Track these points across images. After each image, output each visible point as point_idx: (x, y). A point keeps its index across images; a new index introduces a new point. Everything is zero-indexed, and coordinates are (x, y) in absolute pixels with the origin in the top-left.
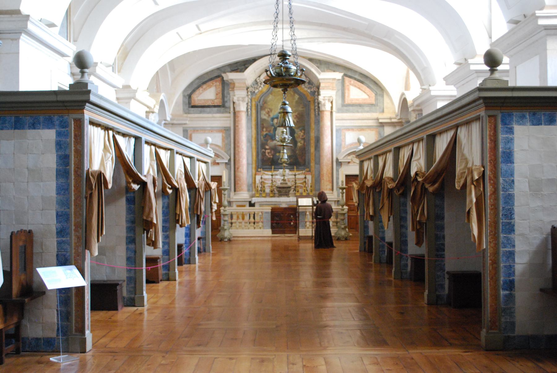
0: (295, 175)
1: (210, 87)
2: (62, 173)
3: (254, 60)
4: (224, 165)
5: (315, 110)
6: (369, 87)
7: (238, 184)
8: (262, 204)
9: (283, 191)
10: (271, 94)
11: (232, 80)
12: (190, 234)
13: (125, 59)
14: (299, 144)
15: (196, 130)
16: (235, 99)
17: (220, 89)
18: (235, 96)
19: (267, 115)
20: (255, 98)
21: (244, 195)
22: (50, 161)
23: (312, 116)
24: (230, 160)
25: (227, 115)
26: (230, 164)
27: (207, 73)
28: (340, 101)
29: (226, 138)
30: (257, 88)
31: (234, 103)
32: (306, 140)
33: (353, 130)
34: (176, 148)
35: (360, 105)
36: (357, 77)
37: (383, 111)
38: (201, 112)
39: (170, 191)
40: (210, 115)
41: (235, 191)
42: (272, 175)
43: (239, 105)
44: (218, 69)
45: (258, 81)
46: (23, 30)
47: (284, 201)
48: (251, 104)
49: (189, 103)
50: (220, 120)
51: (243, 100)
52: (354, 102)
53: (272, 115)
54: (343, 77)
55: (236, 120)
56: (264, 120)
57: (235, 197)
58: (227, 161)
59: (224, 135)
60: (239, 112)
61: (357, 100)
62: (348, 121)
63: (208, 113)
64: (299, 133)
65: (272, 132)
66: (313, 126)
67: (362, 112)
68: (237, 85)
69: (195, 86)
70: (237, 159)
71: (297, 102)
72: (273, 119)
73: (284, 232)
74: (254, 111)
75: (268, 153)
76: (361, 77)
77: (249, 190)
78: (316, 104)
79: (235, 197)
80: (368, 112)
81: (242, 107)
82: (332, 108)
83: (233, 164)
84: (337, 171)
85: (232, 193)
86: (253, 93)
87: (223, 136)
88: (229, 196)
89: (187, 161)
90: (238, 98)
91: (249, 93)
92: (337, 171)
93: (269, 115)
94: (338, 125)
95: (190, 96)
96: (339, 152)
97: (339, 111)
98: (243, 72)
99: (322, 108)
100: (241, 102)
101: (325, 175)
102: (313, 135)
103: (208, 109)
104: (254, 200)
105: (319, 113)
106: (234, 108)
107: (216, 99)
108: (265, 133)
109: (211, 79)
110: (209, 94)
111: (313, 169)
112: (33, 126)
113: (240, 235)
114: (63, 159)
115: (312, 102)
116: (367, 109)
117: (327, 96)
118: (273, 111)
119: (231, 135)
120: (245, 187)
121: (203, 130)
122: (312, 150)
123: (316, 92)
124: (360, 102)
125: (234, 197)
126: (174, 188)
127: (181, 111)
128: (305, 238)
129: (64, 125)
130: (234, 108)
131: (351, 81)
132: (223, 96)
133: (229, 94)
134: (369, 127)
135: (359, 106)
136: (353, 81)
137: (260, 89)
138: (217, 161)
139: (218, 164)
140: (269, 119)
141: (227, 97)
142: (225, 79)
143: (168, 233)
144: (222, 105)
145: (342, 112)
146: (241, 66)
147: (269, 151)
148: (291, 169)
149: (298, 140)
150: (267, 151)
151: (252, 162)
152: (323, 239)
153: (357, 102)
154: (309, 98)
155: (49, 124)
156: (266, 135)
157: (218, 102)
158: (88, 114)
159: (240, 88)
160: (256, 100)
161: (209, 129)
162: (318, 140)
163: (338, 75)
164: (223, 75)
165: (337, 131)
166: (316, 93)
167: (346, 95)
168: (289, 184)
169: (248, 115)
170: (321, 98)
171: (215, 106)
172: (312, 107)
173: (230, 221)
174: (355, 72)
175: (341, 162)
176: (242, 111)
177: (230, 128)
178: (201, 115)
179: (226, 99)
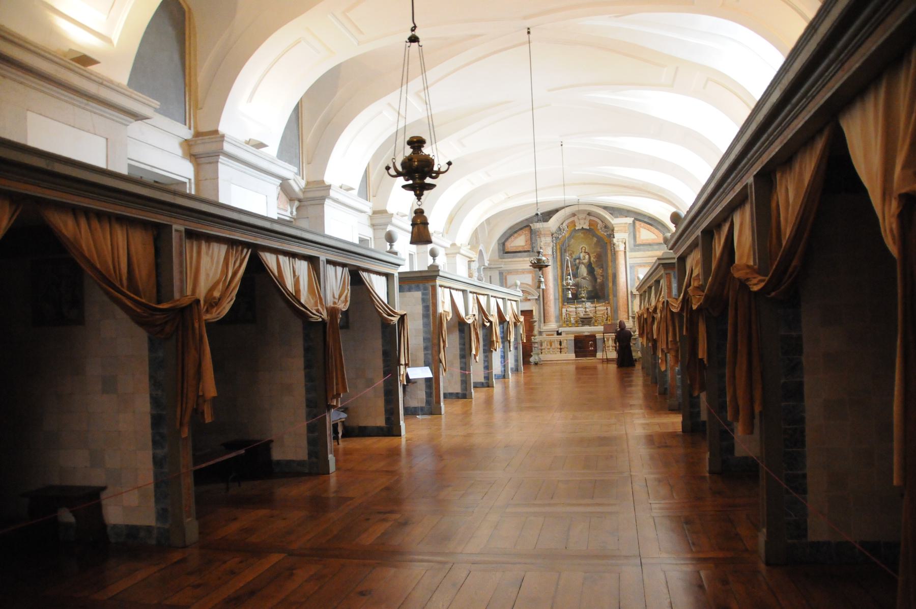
1: (520, 235)
2: (426, 316)
3: (557, 211)
6: (657, 228)
8: (567, 333)
9: (586, 321)
14: (599, 280)
15: (510, 272)
17: (529, 237)
21: (553, 325)
22: (419, 309)
23: (609, 255)
27: (517, 224)
28: (632, 242)
32: (605, 276)
34: (491, 293)
35: (650, 245)
38: (513, 257)
39: (488, 324)
44: (527, 220)
46: (390, 223)
47: (586, 330)
49: (504, 250)
51: (547, 244)
53: (574, 257)
54: (634, 222)
64: (598, 271)
66: (610, 264)
69: (508, 235)
72: (575, 260)
73: (585, 356)
77: (557, 322)
83: (542, 299)
84: (632, 302)
85: (542, 324)
86: (557, 238)
88: (540, 327)
89: (500, 302)
92: (632, 302)
95: (504, 244)
96: (632, 287)
97: (632, 250)
98: (546, 221)
99: (617, 249)
102: (610, 271)
103: (519, 254)
104: (561, 330)
105: (615, 254)
109: (521, 229)
110: (520, 242)
111: (611, 302)
112: (409, 290)
114: (426, 308)
116: (656, 247)
117: (620, 238)
121: (516, 272)
122: (610, 285)
123: (611, 236)
124: (651, 242)
126: (491, 322)
127: (497, 258)
128: (608, 361)
129: (425, 289)
132: (532, 244)
135: (649, 245)
136: (643, 224)
146: (547, 216)
148: (592, 303)
149: (598, 277)
152: (625, 360)
154: (606, 240)
155: (418, 289)
157: (527, 248)
158: (439, 282)
159: (545, 235)
162: (615, 276)
163: (630, 220)
165: (631, 267)
168: (591, 315)
170: (615, 240)
172: (609, 247)
174: (644, 216)
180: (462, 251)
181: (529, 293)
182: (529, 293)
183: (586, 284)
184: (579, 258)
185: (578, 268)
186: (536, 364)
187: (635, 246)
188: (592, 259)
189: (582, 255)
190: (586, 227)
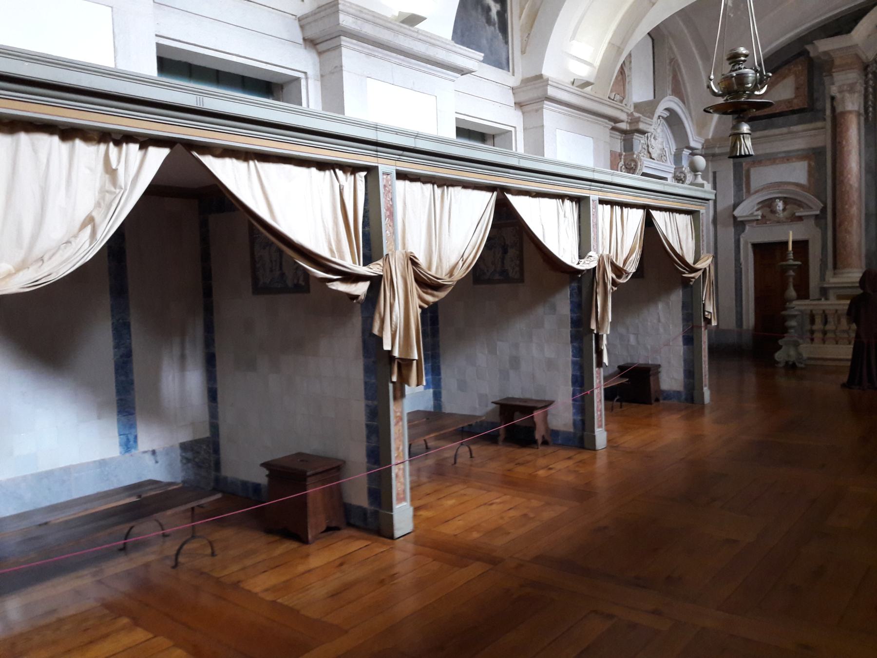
4: (812, 222)
11: (826, 53)
12: (582, 377)
13: (532, 27)
16: (834, 90)
18: (833, 84)
24: (824, 210)
25: (819, 124)
26: (826, 218)
29: (816, 172)
31: (833, 98)
40: (785, 130)
41: (835, 267)
43: (843, 100)
50: (800, 137)
51: (851, 89)
55: (838, 130)
57: (832, 280)
58: (818, 212)
59: (813, 164)
60: (844, 113)
63: (781, 127)
68: (837, 62)
70: (839, 206)
79: (832, 280)
81: (852, 104)
83: (832, 217)
87: (809, 165)
88: (823, 277)
90: (840, 87)
91: (870, 76)
98: (849, 31)
100: (847, 95)
103: (780, 120)
106: (833, 109)
107: (796, 97)
109: (787, 62)
113: (829, 357)
119: (826, 163)
125: (832, 280)
130: (833, 109)
138: (797, 214)
139: (800, 218)
142: (812, 55)
143: (376, 403)
144: (811, 107)
159: (846, 67)
161: (783, 155)
164: (809, 47)
169: (866, 119)
171: (793, 112)
173: (808, 327)
176: (850, 112)
178: (766, 133)
179: (816, 95)
180: (551, 92)
181: (800, 204)
182: (800, 204)
186: (791, 367)
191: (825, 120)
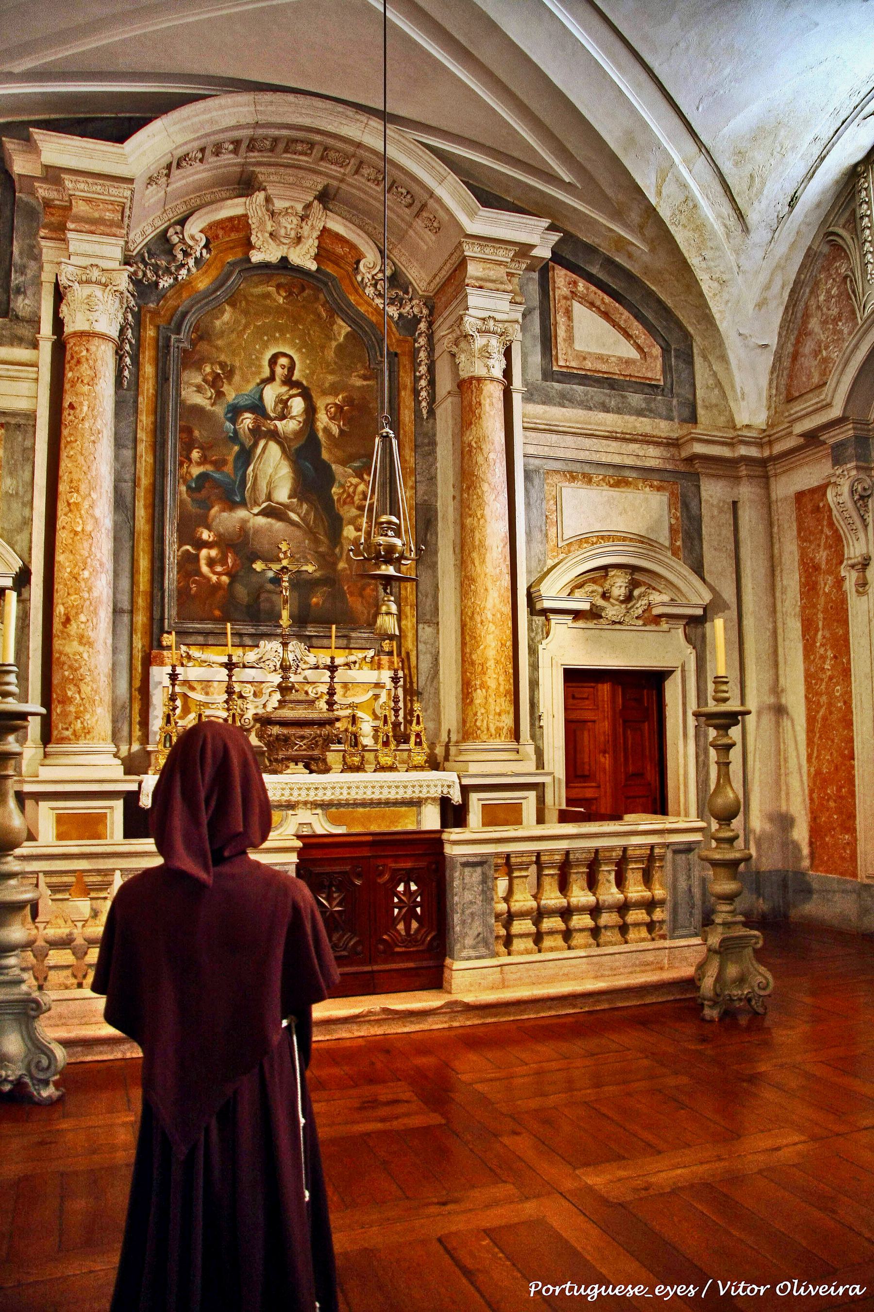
0: (332, 668)
5: (416, 393)
6: (639, 317)
7: (66, 701)
10: (233, 305)
14: (349, 532)
19: (210, 392)
20: (155, 313)
30: (168, 271)
33: (588, 479)
35: (609, 382)
36: (595, 270)
37: (693, 419)
41: (46, 738)
42: (230, 666)
45: (175, 239)
48: (138, 339)
52: (588, 365)
53: (231, 395)
56: (197, 410)
57: (45, 773)
61: (600, 358)
62: (569, 440)
65: (229, 468)
67: (618, 411)
71: (340, 348)
72: (235, 412)
74: (148, 370)
75: (211, 563)
76: (609, 273)
78: (423, 369)
80: (640, 413)
82: (508, 373)
84: (533, 651)
92: (533, 651)
93: (220, 394)
94: (531, 450)
101: (491, 664)
108: (196, 471)
115: (405, 360)
116: (636, 399)
118: (237, 378)
120: (100, 718)
131: (575, 283)
133: (37, 258)
134: (646, 473)
137: (184, 272)
140: (220, 410)
141: (22, 271)
145: (547, 400)
147: (213, 553)
150: (204, 552)
151: (132, 602)
153: (604, 368)
156: (203, 476)
160: (161, 322)
165: (528, 476)
166: (423, 326)
167: (561, 332)
175: (545, 612)
177: (31, 416)
183: (288, 549)
184: (258, 408)
185: (246, 456)
187: (548, 375)
188: (323, 419)
189: (271, 394)
190: (303, 257)
191: (35, 345)
